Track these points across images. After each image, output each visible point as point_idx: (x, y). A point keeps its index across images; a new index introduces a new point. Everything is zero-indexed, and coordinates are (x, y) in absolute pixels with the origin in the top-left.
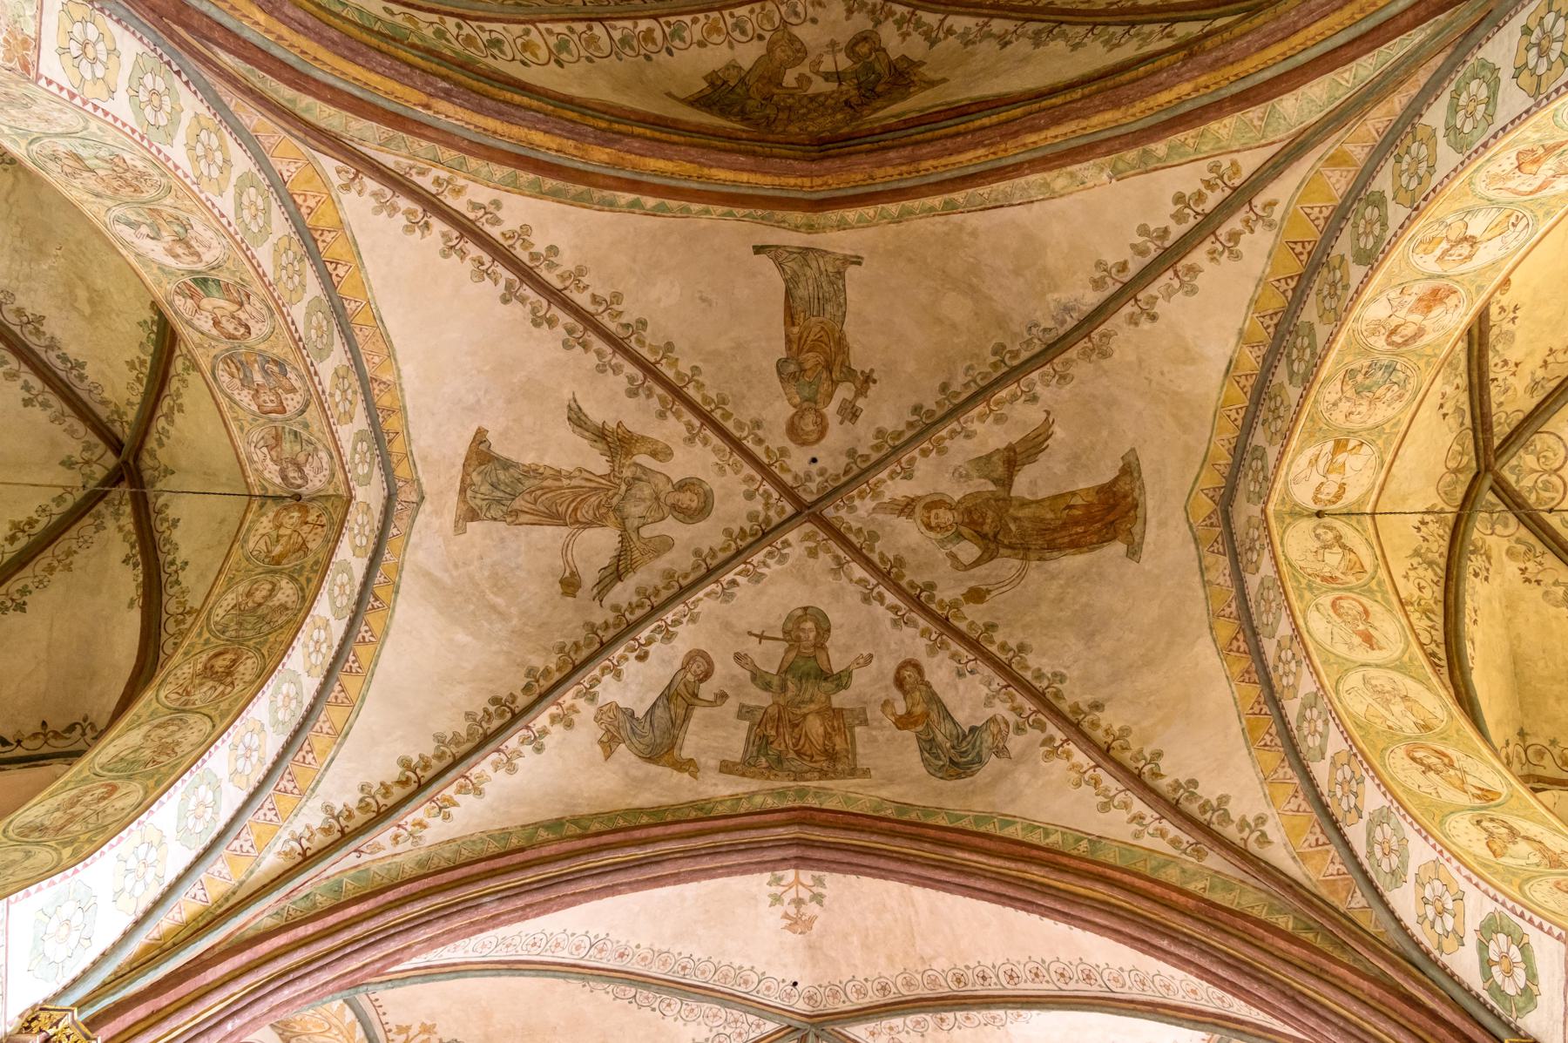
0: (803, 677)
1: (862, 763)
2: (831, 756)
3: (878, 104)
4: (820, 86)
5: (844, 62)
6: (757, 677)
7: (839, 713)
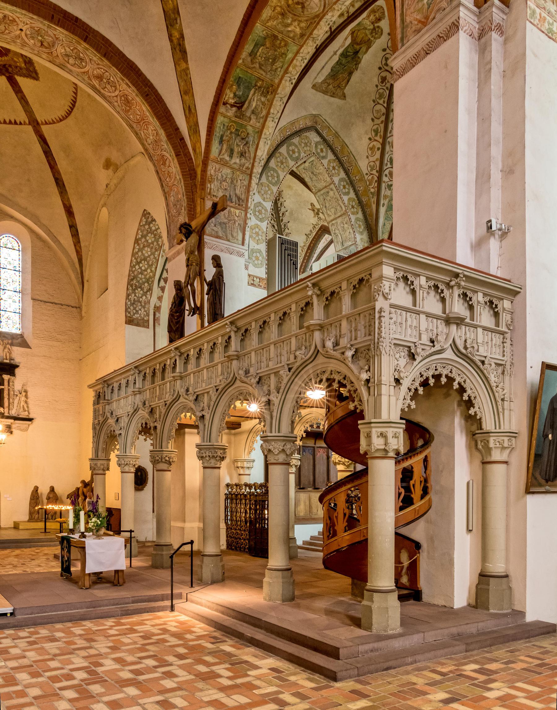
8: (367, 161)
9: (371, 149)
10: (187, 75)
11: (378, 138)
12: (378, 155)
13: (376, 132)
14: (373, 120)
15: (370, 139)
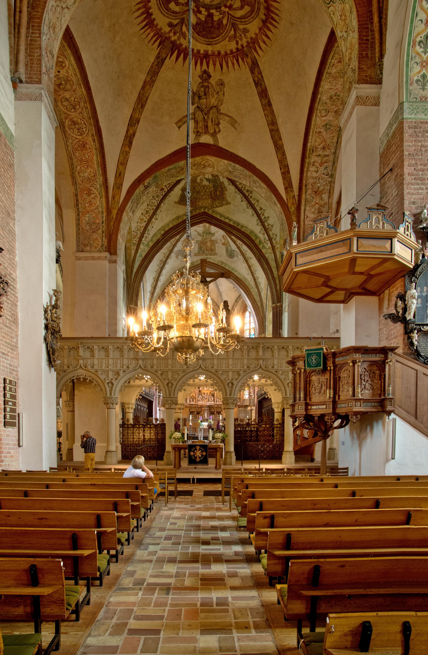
0: (207, 234)
1: (217, 252)
2: (211, 250)
3: (217, 203)
4: (205, 183)
5: (210, 177)
6: (199, 234)
7: (213, 241)
8: (136, 225)
9: (141, 219)
10: (127, 155)
11: (147, 216)
12: (144, 224)
13: (147, 212)
14: (148, 205)
15: (142, 214)
